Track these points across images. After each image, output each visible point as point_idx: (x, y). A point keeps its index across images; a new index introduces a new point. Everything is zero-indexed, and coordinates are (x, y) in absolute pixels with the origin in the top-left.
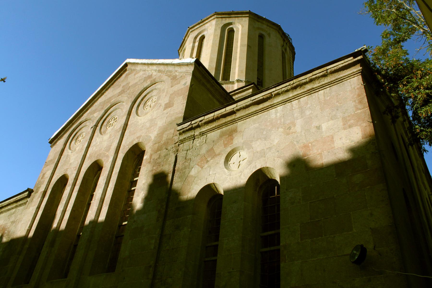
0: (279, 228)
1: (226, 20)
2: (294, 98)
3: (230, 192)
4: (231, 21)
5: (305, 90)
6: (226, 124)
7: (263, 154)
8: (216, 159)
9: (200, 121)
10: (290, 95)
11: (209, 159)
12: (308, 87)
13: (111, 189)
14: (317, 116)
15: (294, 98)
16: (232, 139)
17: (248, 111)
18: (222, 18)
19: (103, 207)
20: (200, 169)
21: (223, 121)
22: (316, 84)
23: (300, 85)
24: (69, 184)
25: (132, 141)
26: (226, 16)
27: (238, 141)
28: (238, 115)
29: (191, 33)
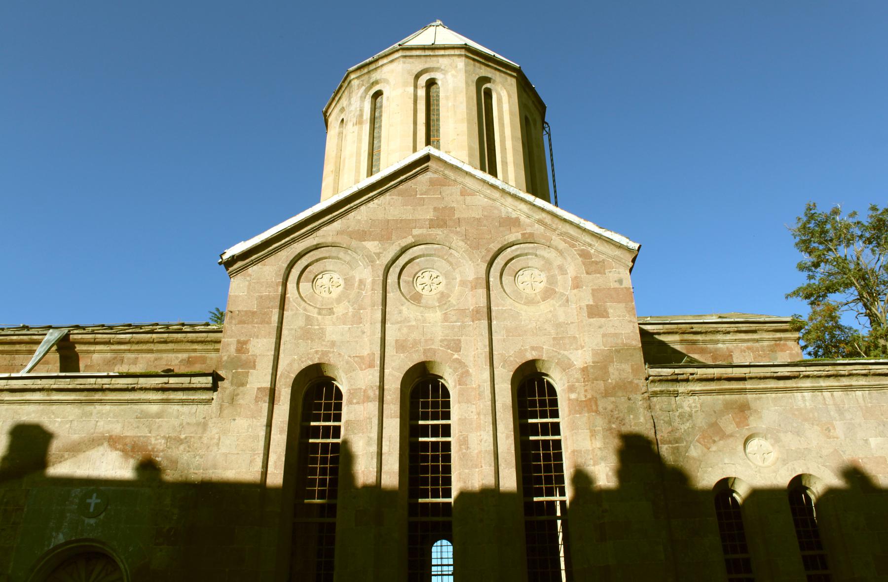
0: (526, 522)
1: (480, 68)
2: (827, 388)
3: (757, 495)
4: (489, 75)
5: (842, 384)
6: (731, 391)
7: (801, 455)
8: (730, 441)
9: (692, 374)
10: (823, 383)
11: (716, 439)
12: (845, 382)
13: (507, 437)
14: (860, 425)
15: (827, 388)
16: (746, 419)
17: (762, 385)
18: (474, 60)
19: (272, 432)
20: (706, 450)
21: (727, 385)
22: (854, 382)
23: (837, 376)
24: (392, 406)
25: (522, 352)
26: (483, 61)
27: (754, 423)
28: (748, 385)
29: (402, 60)
